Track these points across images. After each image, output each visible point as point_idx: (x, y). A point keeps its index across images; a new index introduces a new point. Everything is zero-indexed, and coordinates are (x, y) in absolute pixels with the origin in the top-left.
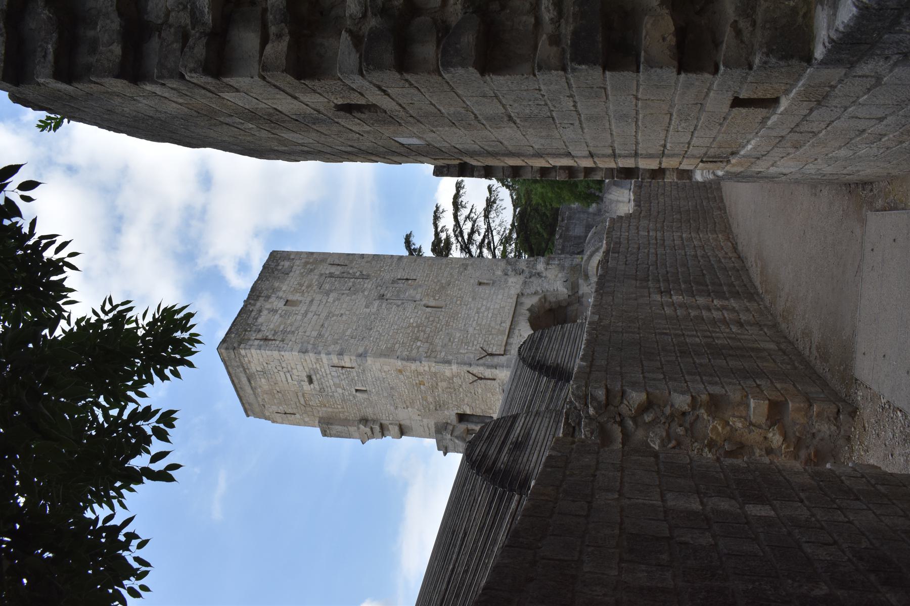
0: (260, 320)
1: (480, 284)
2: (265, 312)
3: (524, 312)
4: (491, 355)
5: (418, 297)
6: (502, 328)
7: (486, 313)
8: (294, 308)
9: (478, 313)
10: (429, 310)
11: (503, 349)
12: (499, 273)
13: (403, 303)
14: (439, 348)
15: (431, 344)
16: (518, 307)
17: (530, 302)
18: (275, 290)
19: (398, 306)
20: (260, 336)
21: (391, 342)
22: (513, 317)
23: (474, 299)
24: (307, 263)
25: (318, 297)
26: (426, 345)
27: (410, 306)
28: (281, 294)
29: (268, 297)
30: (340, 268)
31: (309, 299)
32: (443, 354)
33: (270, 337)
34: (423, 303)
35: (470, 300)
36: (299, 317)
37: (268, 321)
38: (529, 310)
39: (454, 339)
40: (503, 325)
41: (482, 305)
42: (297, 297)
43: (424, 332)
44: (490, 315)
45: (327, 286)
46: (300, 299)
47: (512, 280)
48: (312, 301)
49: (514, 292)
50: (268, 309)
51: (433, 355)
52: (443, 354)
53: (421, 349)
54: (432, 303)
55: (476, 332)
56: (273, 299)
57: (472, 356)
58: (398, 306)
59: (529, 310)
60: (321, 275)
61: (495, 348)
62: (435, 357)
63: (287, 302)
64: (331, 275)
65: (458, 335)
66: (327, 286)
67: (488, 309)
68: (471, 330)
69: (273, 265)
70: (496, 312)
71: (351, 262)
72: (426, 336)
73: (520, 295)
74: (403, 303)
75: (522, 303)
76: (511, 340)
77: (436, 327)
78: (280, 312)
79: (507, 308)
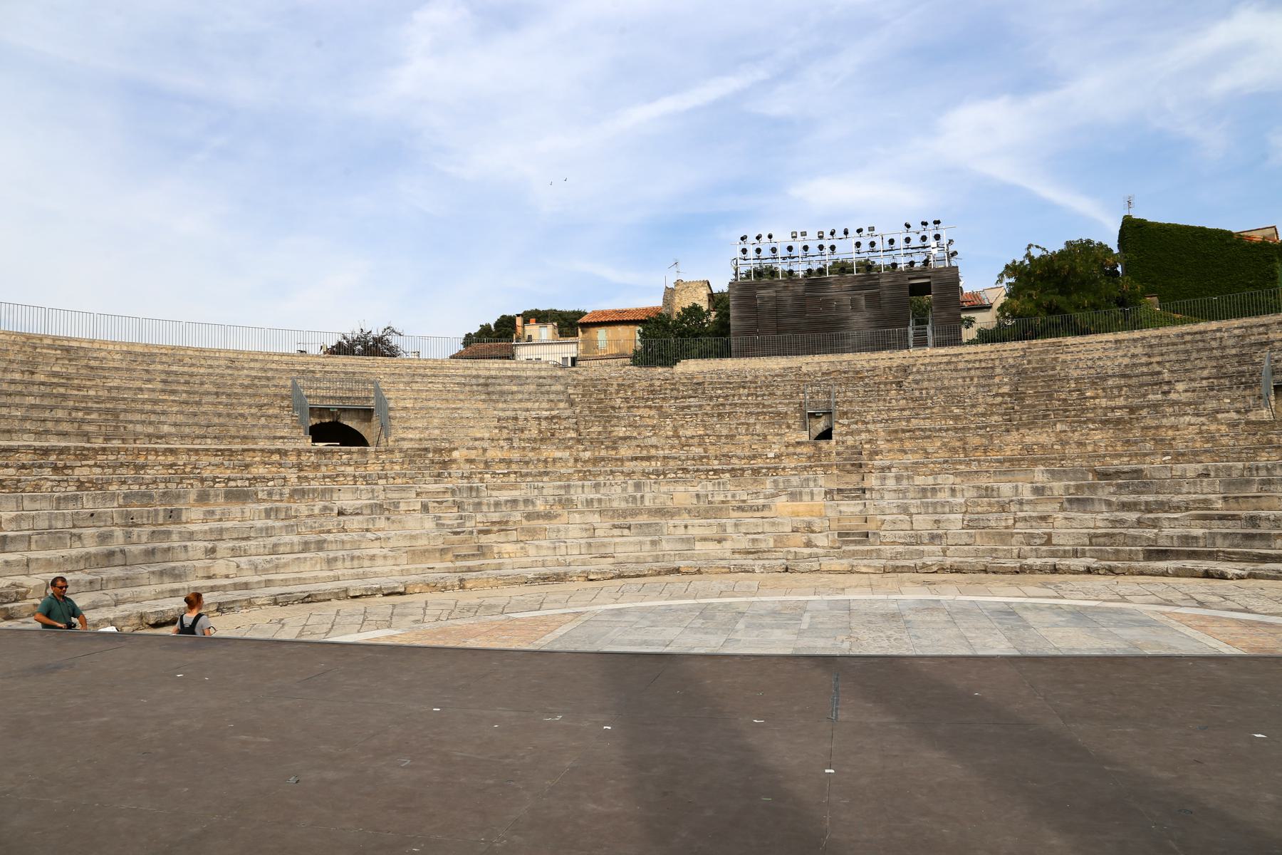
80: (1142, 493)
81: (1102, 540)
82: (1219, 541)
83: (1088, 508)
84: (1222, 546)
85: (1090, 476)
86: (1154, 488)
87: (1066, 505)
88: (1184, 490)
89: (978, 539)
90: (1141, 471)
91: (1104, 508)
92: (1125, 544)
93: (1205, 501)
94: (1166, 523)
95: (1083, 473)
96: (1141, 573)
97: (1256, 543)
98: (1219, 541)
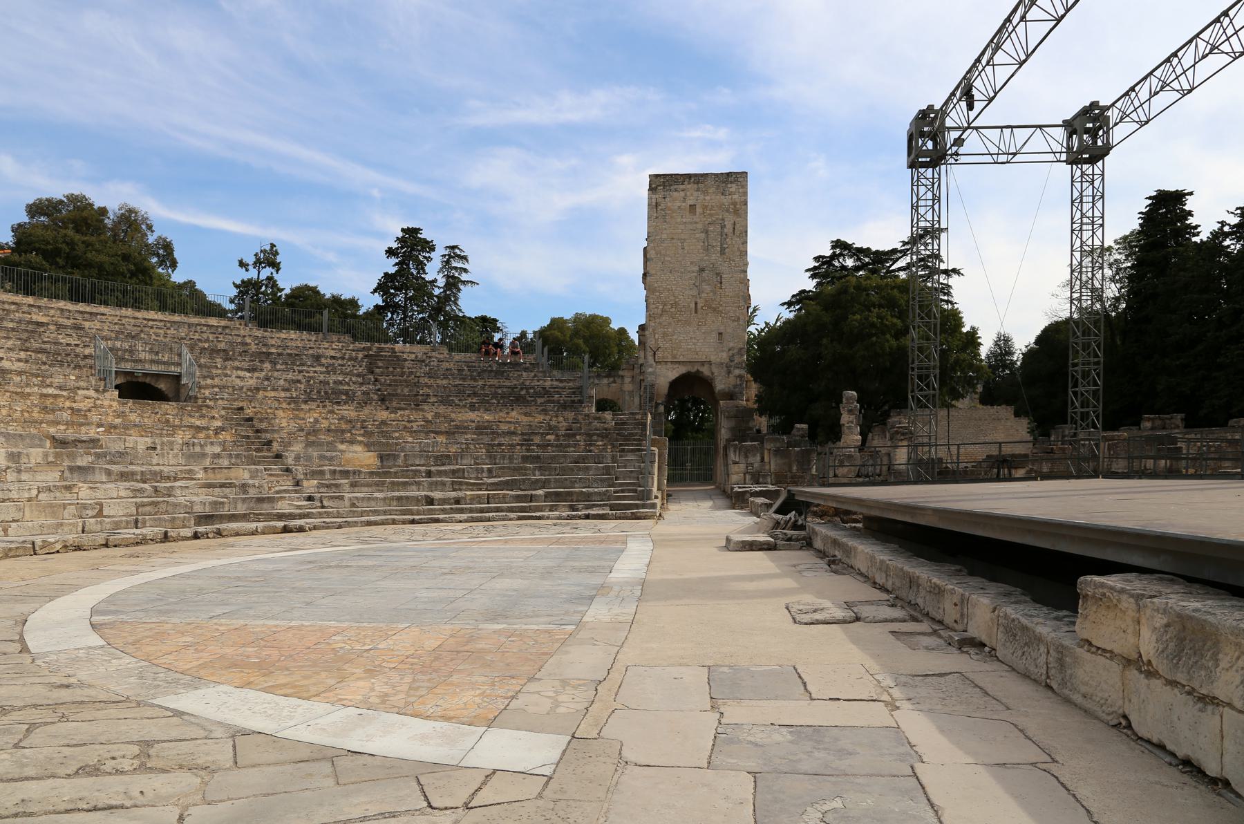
1: (720, 334)
12: (731, 345)
17: (705, 371)
27: (695, 292)
47: (725, 355)
49: (713, 358)
73: (710, 363)
80: (118, 463)
81: (148, 509)
82: (240, 506)
83: (89, 478)
84: (241, 509)
85: (48, 443)
86: (128, 459)
87: (67, 474)
88: (154, 462)
89: (27, 514)
90: (99, 440)
91: (104, 478)
92: (167, 512)
93: (190, 471)
94: (178, 492)
95: (41, 440)
96: (237, 534)
97: (265, 505)
98: (240, 506)
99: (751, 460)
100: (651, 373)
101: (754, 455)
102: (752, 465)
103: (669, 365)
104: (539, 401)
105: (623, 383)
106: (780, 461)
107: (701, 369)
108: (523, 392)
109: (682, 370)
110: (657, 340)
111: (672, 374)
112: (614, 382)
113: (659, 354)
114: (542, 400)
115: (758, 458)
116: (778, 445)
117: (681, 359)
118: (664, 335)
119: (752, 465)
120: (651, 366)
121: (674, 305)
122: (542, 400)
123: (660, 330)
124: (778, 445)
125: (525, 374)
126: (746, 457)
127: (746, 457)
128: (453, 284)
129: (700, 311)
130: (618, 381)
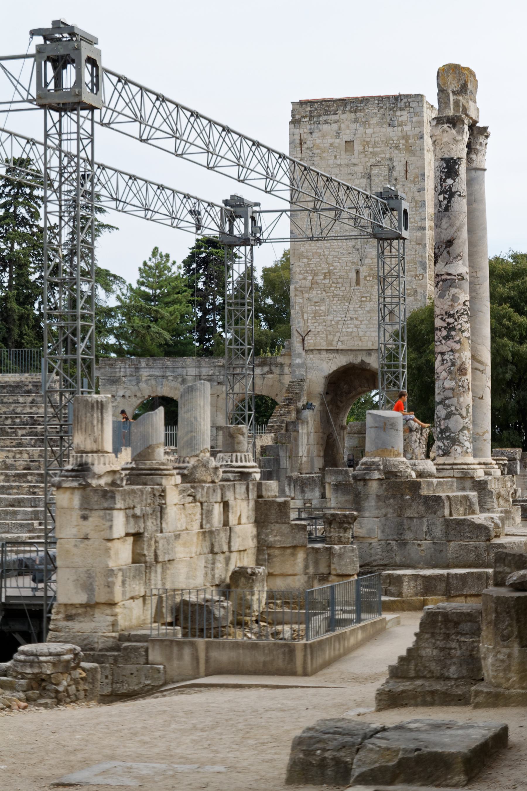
0: (325, 127)
2: (335, 127)
3: (357, 360)
4: (303, 340)
5: (366, 261)
6: (334, 343)
7: (352, 326)
8: (343, 152)
9: (352, 319)
10: (353, 275)
11: (311, 348)
13: (358, 250)
14: (306, 296)
15: (311, 288)
16: (364, 353)
18: (366, 124)
19: (354, 247)
20: (304, 136)
21: (310, 254)
22: (351, 350)
23: (369, 312)
24: (406, 138)
25: (360, 169)
26: (308, 284)
28: (361, 130)
29: (356, 121)
30: (403, 173)
31: (356, 161)
32: (301, 301)
33: (305, 146)
34: (361, 269)
35: (367, 309)
36: (331, 161)
37: (325, 134)
38: (362, 361)
39: (319, 306)
40: (340, 343)
41: (361, 321)
42: (358, 147)
43: (325, 279)
44: (350, 330)
45: (375, 171)
46: (356, 152)
48: (354, 165)
50: (340, 128)
51: (299, 293)
52: (301, 301)
53: (303, 281)
54: (362, 277)
55: (329, 322)
56: (353, 126)
57: (301, 325)
58: (354, 247)
59: (362, 361)
60: (391, 159)
61: (312, 341)
62: (296, 295)
63: (349, 143)
64: (391, 169)
65: (323, 308)
66: (375, 171)
67: (356, 327)
68: (330, 317)
69: (402, 104)
70: (354, 334)
71: (414, 182)
72: (320, 281)
74: (358, 250)
75: (370, 354)
76: (325, 353)
77: (331, 286)
78: (337, 141)
79: (360, 343)
99: (308, 495)
100: (299, 366)
101: (312, 490)
102: (310, 501)
103: (324, 355)
104: (20, 432)
105: (282, 374)
106: (342, 498)
107: (367, 360)
108: (9, 422)
109: (341, 361)
110: (306, 322)
111: (329, 365)
112: (271, 372)
113: (310, 341)
114: (24, 432)
115: (317, 493)
116: (340, 478)
117: (340, 346)
118: (316, 315)
119: (310, 501)
120: (299, 356)
121: (328, 274)
122: (24, 432)
123: (310, 308)
124: (340, 478)
125: (21, 399)
126: (303, 492)
127: (303, 492)
128: (86, 226)
129: (362, 282)
130: (277, 370)
